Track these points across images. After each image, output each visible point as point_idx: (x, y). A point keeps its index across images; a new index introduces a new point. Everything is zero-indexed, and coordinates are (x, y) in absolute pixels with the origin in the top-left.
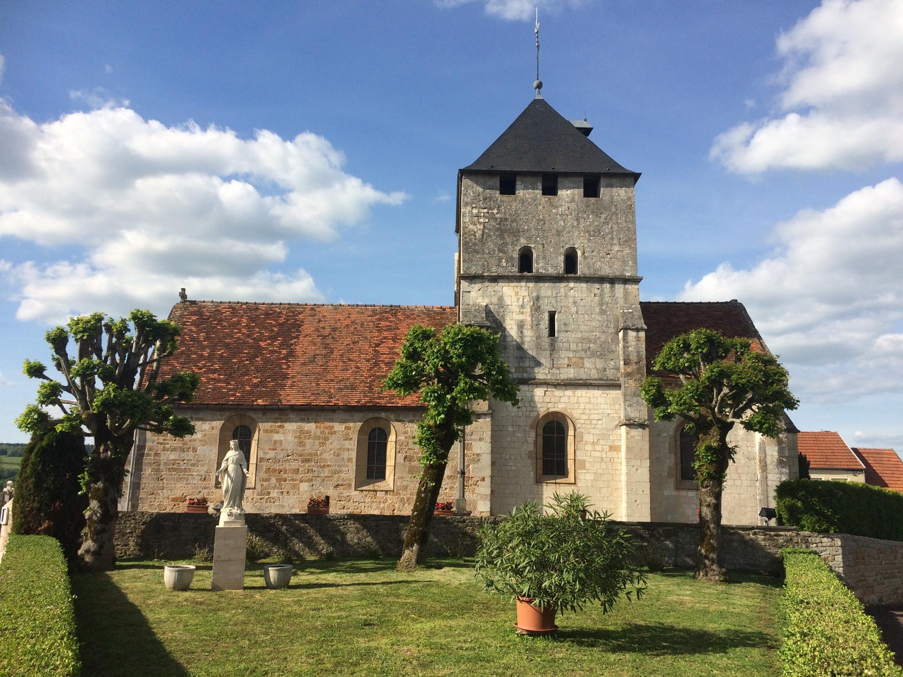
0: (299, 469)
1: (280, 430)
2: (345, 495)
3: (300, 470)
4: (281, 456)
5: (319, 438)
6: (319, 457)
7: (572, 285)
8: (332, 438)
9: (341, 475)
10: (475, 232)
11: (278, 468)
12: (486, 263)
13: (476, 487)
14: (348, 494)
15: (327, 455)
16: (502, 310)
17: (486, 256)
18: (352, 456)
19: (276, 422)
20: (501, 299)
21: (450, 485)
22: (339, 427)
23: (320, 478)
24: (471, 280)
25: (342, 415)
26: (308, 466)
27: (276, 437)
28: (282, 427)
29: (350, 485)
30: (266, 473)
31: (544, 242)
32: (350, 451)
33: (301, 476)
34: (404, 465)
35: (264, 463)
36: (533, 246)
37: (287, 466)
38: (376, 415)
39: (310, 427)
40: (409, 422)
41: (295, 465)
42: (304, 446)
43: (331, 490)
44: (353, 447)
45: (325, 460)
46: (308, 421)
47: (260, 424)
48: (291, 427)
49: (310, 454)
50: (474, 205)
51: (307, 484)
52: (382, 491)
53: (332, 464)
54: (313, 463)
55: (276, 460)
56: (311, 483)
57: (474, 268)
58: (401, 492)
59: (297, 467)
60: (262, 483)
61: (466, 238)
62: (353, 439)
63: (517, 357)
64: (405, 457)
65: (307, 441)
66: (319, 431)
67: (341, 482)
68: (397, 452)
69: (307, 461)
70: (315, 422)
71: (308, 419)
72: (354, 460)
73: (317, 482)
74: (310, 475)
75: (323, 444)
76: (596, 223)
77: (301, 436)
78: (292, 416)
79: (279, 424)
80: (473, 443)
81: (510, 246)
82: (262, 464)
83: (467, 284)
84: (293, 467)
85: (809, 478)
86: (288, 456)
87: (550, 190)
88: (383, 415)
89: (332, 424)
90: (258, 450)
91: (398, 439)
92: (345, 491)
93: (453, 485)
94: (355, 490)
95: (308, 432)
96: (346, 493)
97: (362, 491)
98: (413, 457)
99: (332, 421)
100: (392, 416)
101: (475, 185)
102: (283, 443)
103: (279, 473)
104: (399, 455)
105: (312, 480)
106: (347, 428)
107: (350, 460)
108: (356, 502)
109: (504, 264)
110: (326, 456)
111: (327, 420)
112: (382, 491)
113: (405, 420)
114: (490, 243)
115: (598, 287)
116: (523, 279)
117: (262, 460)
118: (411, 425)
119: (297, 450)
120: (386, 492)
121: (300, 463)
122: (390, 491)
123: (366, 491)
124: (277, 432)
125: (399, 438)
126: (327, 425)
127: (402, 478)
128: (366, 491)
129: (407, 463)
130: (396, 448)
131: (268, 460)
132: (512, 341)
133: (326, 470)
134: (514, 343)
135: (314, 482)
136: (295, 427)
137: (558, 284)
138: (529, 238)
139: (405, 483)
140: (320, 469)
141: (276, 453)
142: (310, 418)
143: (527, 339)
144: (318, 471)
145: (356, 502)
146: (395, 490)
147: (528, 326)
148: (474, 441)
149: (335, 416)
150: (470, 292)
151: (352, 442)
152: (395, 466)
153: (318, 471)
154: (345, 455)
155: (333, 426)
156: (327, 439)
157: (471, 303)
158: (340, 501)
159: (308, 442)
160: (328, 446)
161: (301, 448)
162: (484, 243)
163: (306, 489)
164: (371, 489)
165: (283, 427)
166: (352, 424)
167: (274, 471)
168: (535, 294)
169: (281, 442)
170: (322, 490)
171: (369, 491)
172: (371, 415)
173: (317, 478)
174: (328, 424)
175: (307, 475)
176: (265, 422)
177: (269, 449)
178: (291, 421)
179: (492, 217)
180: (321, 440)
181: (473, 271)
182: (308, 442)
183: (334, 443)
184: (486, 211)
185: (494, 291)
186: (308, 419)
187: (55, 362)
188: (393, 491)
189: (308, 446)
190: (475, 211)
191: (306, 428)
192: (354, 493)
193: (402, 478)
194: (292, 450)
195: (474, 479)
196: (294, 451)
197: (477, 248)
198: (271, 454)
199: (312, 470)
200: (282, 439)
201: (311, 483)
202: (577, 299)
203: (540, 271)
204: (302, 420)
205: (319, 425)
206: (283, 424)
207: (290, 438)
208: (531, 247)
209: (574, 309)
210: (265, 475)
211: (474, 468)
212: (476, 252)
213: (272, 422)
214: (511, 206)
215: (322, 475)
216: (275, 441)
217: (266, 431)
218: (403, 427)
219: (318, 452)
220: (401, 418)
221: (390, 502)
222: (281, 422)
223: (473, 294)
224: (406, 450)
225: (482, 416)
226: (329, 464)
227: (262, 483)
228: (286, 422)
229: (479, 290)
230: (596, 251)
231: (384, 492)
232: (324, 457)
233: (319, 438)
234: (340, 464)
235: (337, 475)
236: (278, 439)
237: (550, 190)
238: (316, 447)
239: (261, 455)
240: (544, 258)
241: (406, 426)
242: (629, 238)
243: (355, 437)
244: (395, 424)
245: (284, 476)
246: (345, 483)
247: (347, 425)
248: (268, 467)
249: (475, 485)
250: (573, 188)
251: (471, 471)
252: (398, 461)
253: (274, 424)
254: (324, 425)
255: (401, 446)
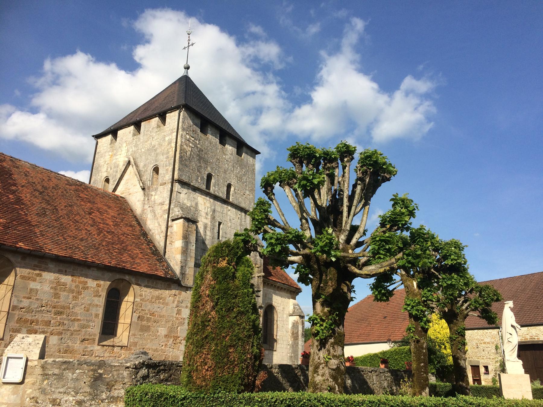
0: (51, 321)
1: (38, 278)
2: (89, 349)
3: (52, 322)
4: (34, 306)
5: (72, 291)
6: (71, 310)
7: (229, 208)
8: (85, 293)
9: (88, 330)
10: (187, 151)
11: (30, 318)
12: (190, 176)
13: (180, 345)
14: (91, 349)
15: (79, 309)
16: (197, 213)
17: (191, 171)
18: (99, 313)
19: (34, 270)
20: (197, 204)
21: (165, 343)
22: (92, 283)
23: (69, 332)
24: (182, 184)
25: (96, 273)
26: (60, 319)
27: (33, 285)
28: (40, 275)
29: (94, 340)
30: (17, 323)
31: (219, 174)
32: (98, 308)
33: (52, 328)
34: (137, 324)
35: (17, 312)
36: (213, 174)
37: (39, 317)
38: (122, 277)
39: (66, 279)
40: (144, 287)
41: (47, 317)
42: (59, 298)
43: (78, 344)
44: (100, 303)
45: (77, 314)
46: (66, 274)
47: (18, 269)
48: (49, 276)
49: (63, 307)
50: (187, 132)
51: (56, 337)
52: (119, 346)
53: (82, 318)
54: (65, 316)
55: (29, 310)
56: (61, 337)
57: (184, 176)
58: (132, 347)
59: (49, 319)
60: (11, 333)
61: (182, 153)
62: (102, 296)
63: (202, 249)
64: (139, 317)
65: (62, 293)
66: (74, 285)
67: (87, 337)
68: (134, 311)
69: (60, 313)
70: (72, 276)
71: (66, 271)
72: (101, 316)
73: (66, 336)
74: (61, 328)
75: (75, 298)
76: (241, 173)
77: (57, 286)
78: (51, 266)
79: (38, 272)
80: (183, 310)
81: (203, 169)
82: (14, 312)
83: (180, 187)
84: (46, 319)
85: (451, 366)
86: (42, 307)
87: (222, 142)
88: (127, 278)
89: (86, 280)
90: (11, 297)
91: (135, 300)
92: (89, 346)
93: (167, 343)
94: (98, 345)
95: (65, 284)
96: (90, 348)
97: (103, 346)
98: (144, 317)
99: (86, 276)
100: (133, 280)
101: (189, 119)
102: (39, 293)
103: (31, 324)
104: (134, 314)
105: (61, 333)
106: (98, 286)
107: (97, 316)
108: (97, 356)
109: (200, 181)
110: (77, 310)
111: (82, 275)
112: (119, 346)
113: (143, 285)
114: (193, 163)
115: (240, 213)
116: (208, 195)
117: (15, 308)
118: (145, 289)
119: (52, 301)
120: (122, 347)
121: (52, 315)
122: (125, 346)
123: (106, 346)
124: (34, 280)
125: (136, 300)
126: (82, 280)
127: (134, 335)
128: (106, 346)
129: (140, 322)
130: (133, 308)
131: (21, 308)
132: (200, 237)
133: (76, 324)
134: (201, 238)
135: (63, 336)
136: (53, 278)
137: (223, 205)
138: (212, 168)
139: (136, 340)
140: (71, 323)
141: (31, 302)
142: (68, 270)
143: (208, 237)
144: (69, 324)
145: (97, 356)
146: (128, 346)
147: (208, 229)
148: (183, 308)
149: (90, 272)
150: (180, 193)
151: (101, 299)
152: (130, 325)
153: (69, 324)
154: (93, 311)
155: (87, 282)
156: (79, 293)
157: (181, 201)
158: (84, 355)
159: (63, 294)
160: (80, 300)
161: (56, 300)
162: (190, 161)
163: (55, 343)
164: (110, 344)
165: (40, 275)
166: (102, 282)
167: (26, 321)
168: (213, 208)
169: (37, 290)
170: (70, 344)
171: (109, 346)
172: (118, 276)
173: (66, 331)
174: (83, 279)
175: (58, 328)
176: (24, 267)
177: (24, 297)
178: (49, 271)
179: (196, 145)
180: (74, 294)
181: (185, 179)
182: (63, 294)
183: (86, 298)
184: (193, 139)
185: (194, 198)
186: (66, 271)
187: (394, 279)
188: (127, 347)
189: (62, 299)
190: (188, 137)
191: (63, 281)
192: (97, 348)
193: (134, 335)
194: (46, 301)
195: (180, 338)
196: (49, 302)
197: (187, 163)
198: (25, 303)
199: (63, 323)
200: (38, 287)
201: (61, 337)
202: (232, 219)
203: (216, 193)
204: (60, 272)
205: (74, 279)
206: (41, 272)
207: (47, 288)
208: (212, 175)
209: (230, 224)
210: (16, 324)
211: (180, 329)
212: (186, 165)
213: (31, 269)
214: (205, 143)
215: (71, 329)
216: (31, 290)
217: (23, 277)
218: (140, 291)
219: (71, 305)
220: (139, 283)
221: (123, 356)
222: (40, 270)
223: (182, 196)
224: (140, 310)
225: (189, 289)
226: (79, 318)
227: (11, 333)
228: (45, 271)
229: (186, 194)
230: (240, 190)
231: (120, 348)
232: (75, 311)
233: (72, 291)
234: (88, 319)
235: (84, 330)
236: (34, 287)
237: (222, 142)
238: (70, 300)
239: (15, 302)
240: (218, 185)
241: (142, 289)
242: (253, 189)
243: (104, 294)
244: (135, 286)
245: (36, 327)
246: (91, 338)
247: (98, 282)
248: (20, 317)
249: (180, 343)
250: (233, 147)
251: (179, 331)
252: (133, 320)
253: (33, 271)
254: (80, 280)
255: (137, 306)
